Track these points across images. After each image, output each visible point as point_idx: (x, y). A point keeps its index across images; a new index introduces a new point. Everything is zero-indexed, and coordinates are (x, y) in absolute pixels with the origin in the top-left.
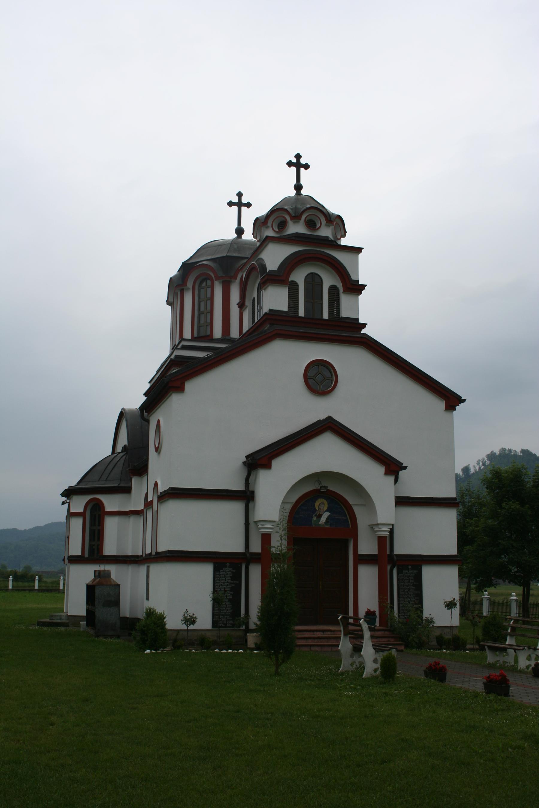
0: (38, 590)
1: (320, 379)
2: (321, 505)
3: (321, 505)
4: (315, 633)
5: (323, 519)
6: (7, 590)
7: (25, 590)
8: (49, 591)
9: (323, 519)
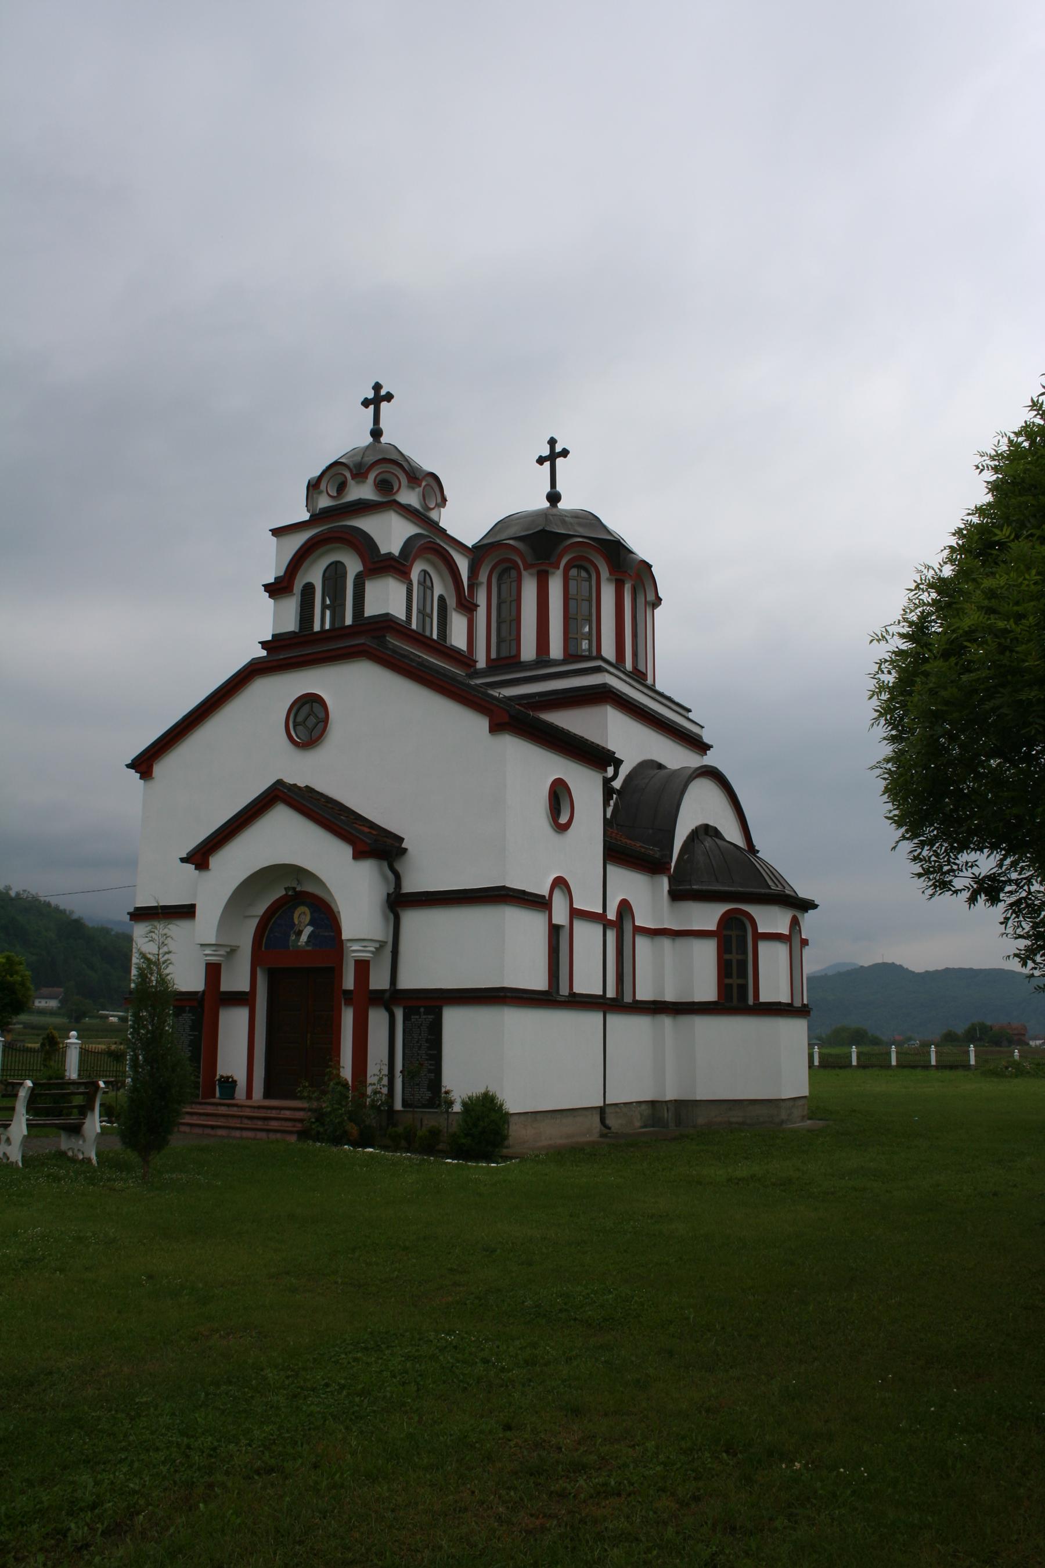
0: (937, 1067)
1: (308, 722)
2: (302, 916)
3: (302, 916)
4: (283, 1112)
5: (304, 938)
6: (927, 1066)
7: (914, 1067)
8: (952, 1067)
9: (304, 938)
